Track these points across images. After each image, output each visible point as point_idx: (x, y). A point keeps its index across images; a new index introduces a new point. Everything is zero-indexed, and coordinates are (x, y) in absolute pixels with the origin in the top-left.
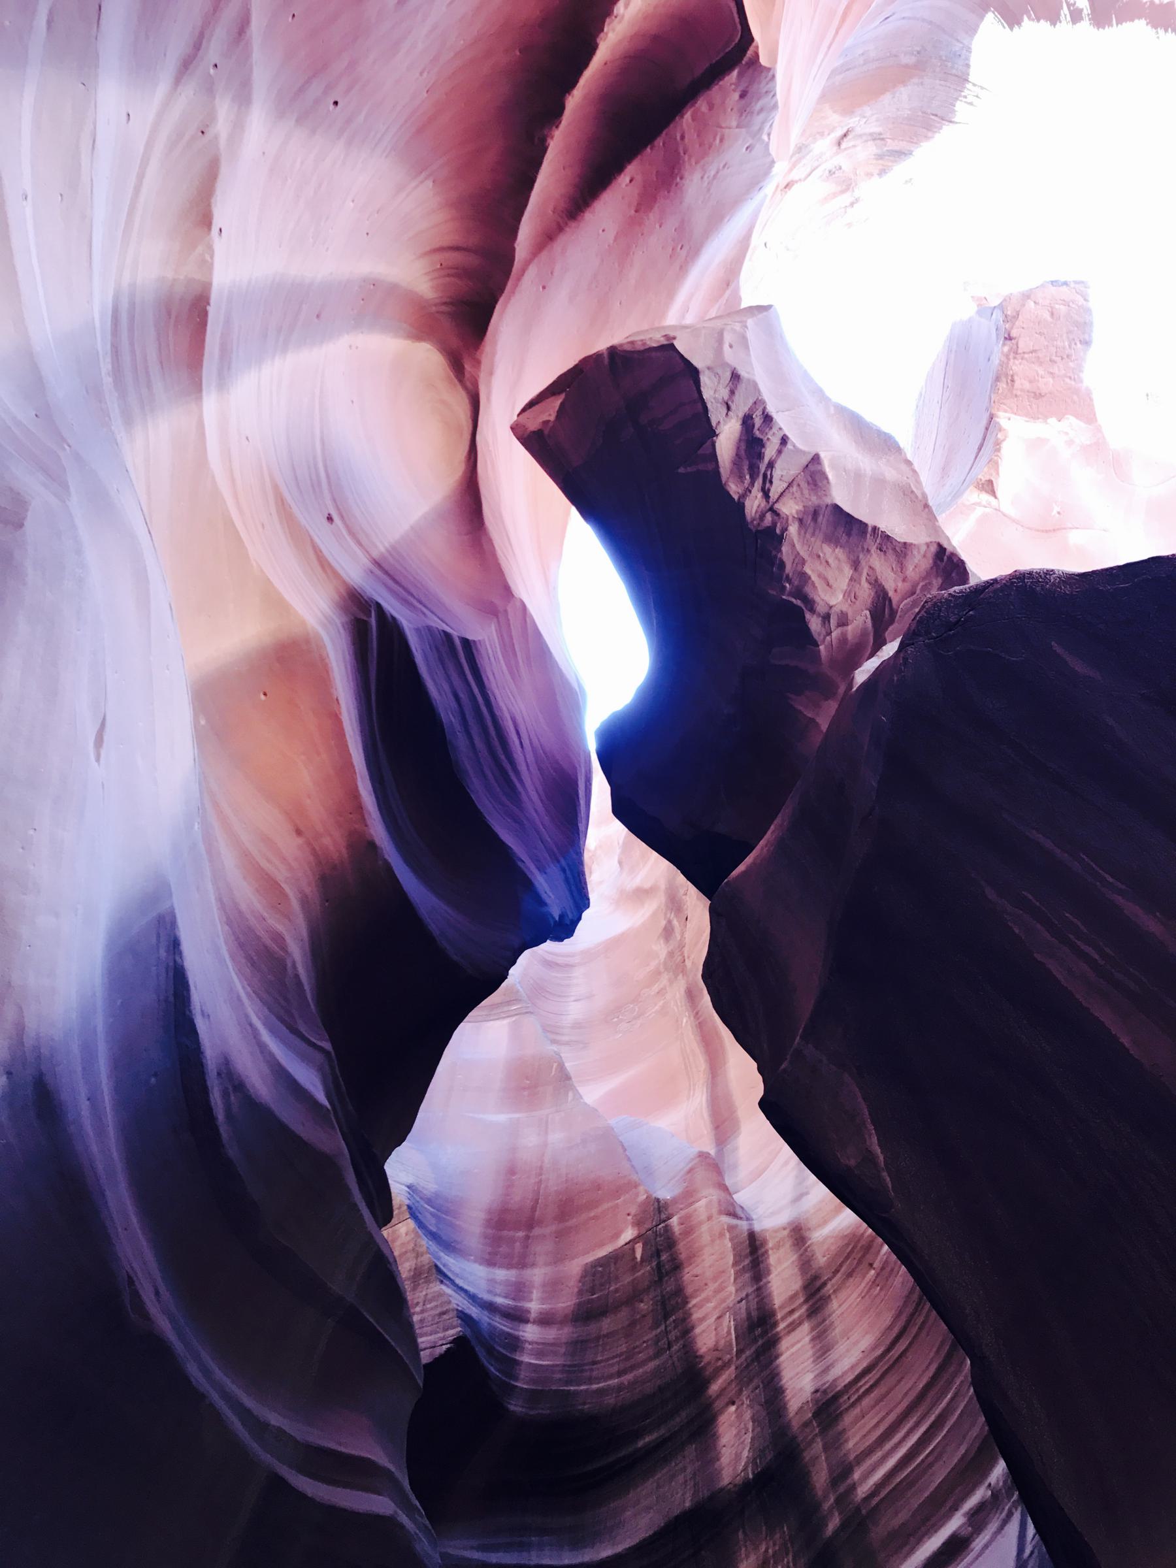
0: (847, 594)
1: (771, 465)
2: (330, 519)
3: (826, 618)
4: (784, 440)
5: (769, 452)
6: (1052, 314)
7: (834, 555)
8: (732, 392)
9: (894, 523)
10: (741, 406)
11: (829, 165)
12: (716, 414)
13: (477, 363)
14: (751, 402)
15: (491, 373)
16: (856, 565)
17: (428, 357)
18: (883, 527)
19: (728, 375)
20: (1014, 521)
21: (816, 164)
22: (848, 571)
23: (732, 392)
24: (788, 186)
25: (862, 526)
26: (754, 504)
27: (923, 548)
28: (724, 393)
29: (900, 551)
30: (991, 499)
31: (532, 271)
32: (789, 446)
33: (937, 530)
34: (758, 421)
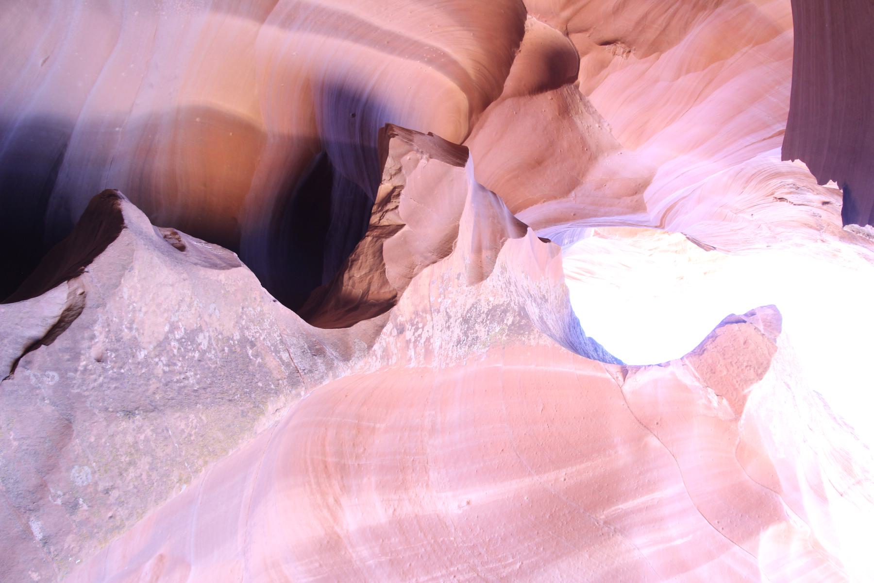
0: (361, 278)
1: (387, 211)
2: (354, 115)
3: (350, 278)
4: (397, 207)
5: (390, 206)
6: (745, 343)
7: (370, 260)
8: (395, 174)
9: (393, 271)
10: (396, 181)
11: (815, 210)
12: (385, 176)
13: (478, 119)
14: (400, 184)
15: (481, 127)
16: (371, 270)
17: (462, 100)
18: (387, 267)
19: (398, 166)
20: (625, 399)
21: (806, 203)
22: (367, 270)
23: (395, 174)
24: (781, 199)
25: (382, 259)
26: (374, 219)
27: (391, 289)
28: (393, 172)
29: (385, 282)
30: (621, 378)
31: (509, 102)
32: (396, 211)
33: (403, 289)
34: (395, 194)
